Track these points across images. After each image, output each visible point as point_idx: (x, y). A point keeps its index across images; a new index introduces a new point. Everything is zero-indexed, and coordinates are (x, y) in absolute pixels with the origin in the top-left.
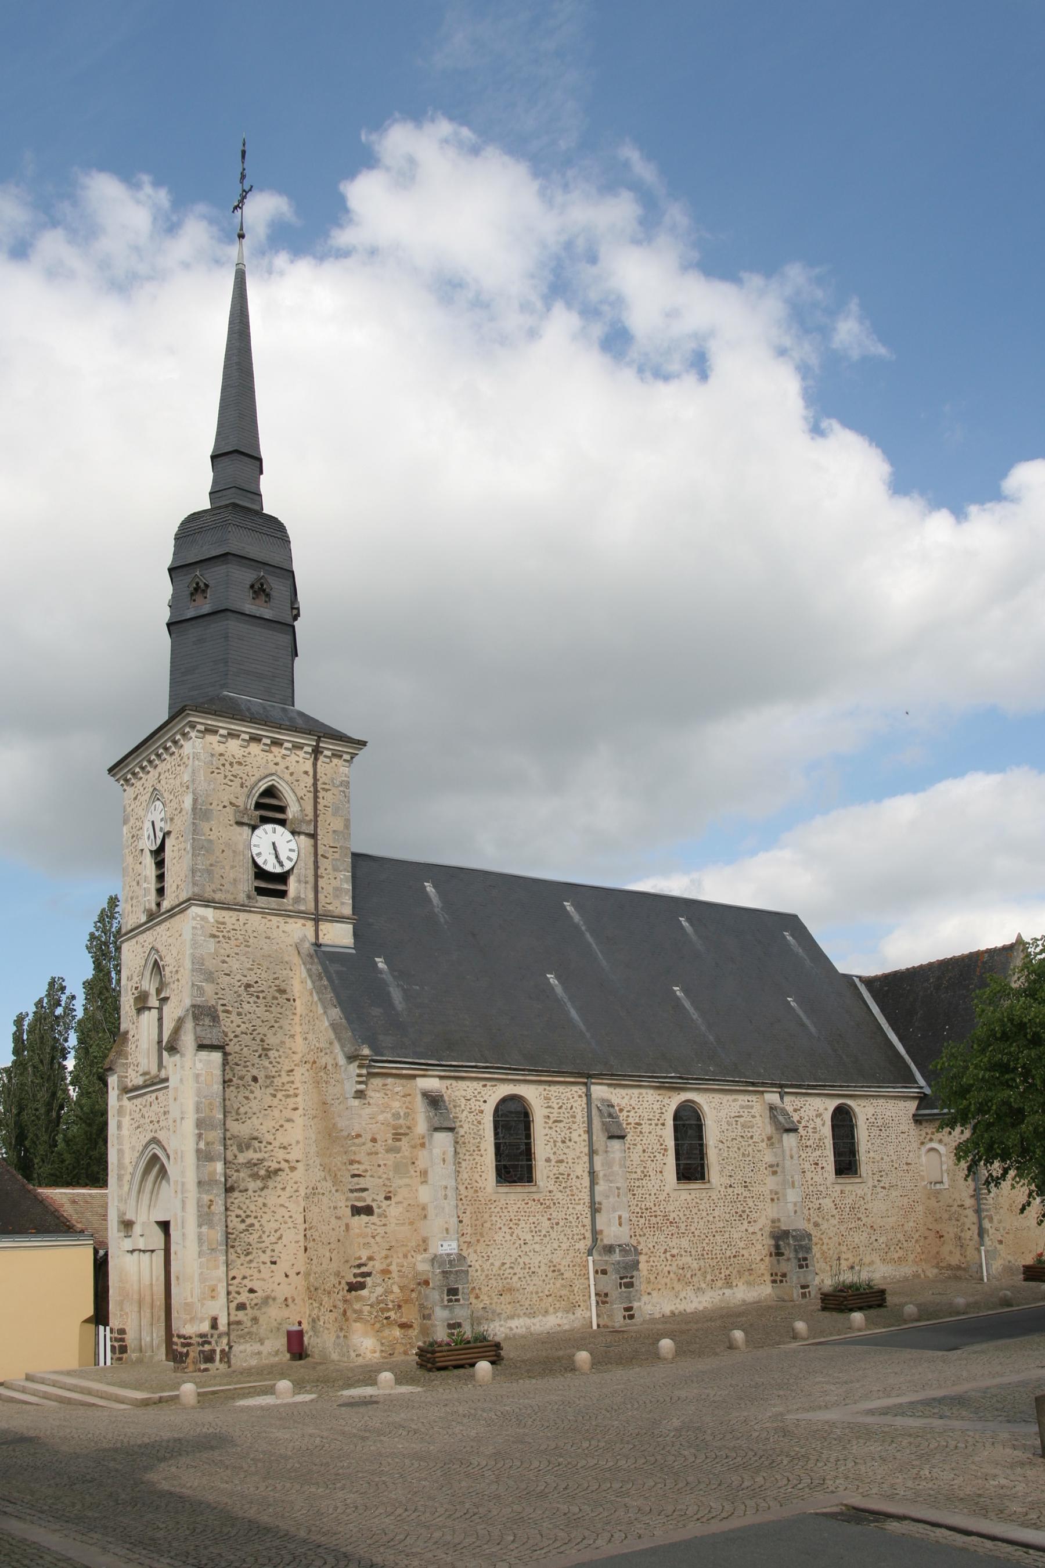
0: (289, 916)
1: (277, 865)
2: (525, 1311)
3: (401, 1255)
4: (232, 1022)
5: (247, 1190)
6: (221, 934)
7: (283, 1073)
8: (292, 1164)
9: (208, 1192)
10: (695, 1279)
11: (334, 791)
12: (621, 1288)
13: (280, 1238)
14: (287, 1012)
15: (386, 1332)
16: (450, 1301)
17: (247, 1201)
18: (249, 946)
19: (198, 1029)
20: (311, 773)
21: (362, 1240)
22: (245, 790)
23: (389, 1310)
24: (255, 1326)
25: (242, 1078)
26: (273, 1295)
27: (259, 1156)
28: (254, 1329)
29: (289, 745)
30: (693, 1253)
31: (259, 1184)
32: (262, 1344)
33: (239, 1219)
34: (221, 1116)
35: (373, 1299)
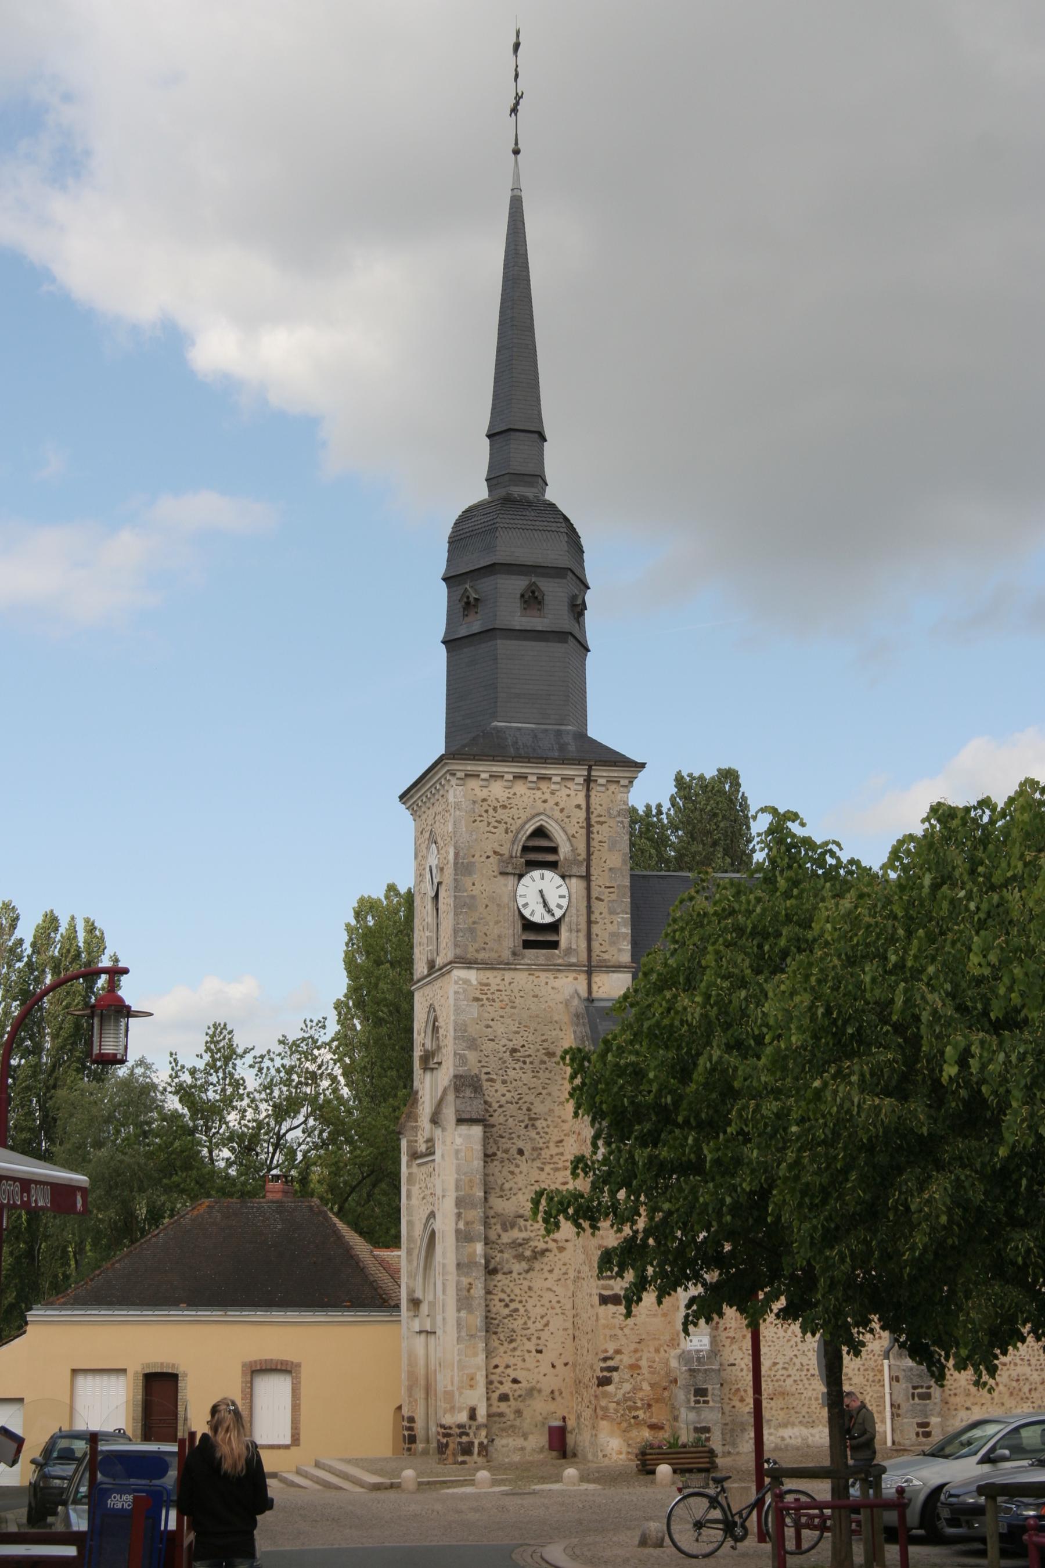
0: (559, 970)
1: (545, 914)
2: (801, 1419)
3: (652, 1349)
4: (496, 1091)
5: (511, 1272)
6: (484, 997)
7: (552, 1145)
8: (560, 1244)
9: (467, 1275)
10: (1034, 1394)
11: (612, 823)
12: (913, 1399)
13: (547, 1325)
14: (556, 1078)
15: (634, 1433)
16: (697, 1402)
17: (511, 1284)
18: (515, 1008)
19: (459, 1101)
20: (584, 806)
21: (608, 1332)
22: (511, 835)
23: (637, 1409)
24: (519, 1420)
25: (506, 1151)
26: (538, 1386)
27: (524, 1235)
28: (517, 1423)
29: (557, 779)
30: (1033, 1361)
31: (524, 1265)
32: (526, 1439)
33: (503, 1304)
34: (482, 1194)
35: (620, 1396)
